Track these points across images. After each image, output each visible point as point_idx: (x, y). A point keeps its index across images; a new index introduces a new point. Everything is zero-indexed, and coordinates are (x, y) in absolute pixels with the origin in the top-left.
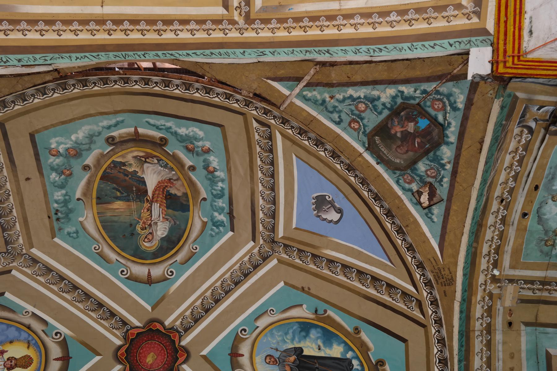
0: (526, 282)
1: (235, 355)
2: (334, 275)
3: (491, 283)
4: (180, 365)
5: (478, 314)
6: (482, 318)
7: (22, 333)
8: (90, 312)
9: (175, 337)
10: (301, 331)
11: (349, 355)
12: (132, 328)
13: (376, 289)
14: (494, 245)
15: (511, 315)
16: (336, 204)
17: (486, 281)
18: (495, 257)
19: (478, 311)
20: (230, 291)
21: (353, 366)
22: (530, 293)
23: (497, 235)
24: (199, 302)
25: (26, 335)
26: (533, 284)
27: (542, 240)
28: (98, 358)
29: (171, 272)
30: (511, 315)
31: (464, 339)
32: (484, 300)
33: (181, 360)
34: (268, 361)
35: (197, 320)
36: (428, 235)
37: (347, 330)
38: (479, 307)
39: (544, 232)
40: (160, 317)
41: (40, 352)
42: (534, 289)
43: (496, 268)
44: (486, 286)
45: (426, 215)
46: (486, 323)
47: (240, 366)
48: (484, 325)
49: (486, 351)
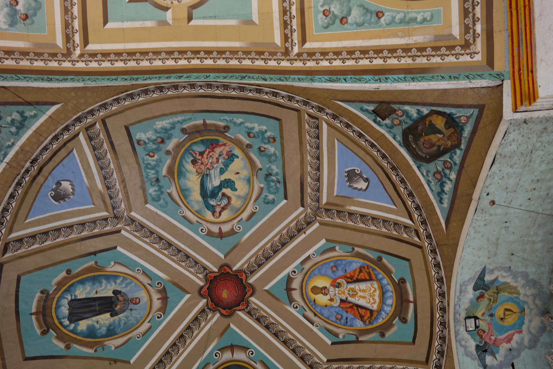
1: (164, 299)
4: (205, 285)
7: (319, 311)
8: (274, 322)
9: (212, 305)
11: (72, 326)
12: (244, 310)
20: (172, 346)
21: (68, 320)
24: (196, 333)
25: (316, 309)
28: (267, 288)
29: (216, 356)
33: (205, 289)
34: (138, 300)
35: (196, 319)
37: (76, 343)
40: (223, 319)
41: (307, 296)
47: (159, 292)
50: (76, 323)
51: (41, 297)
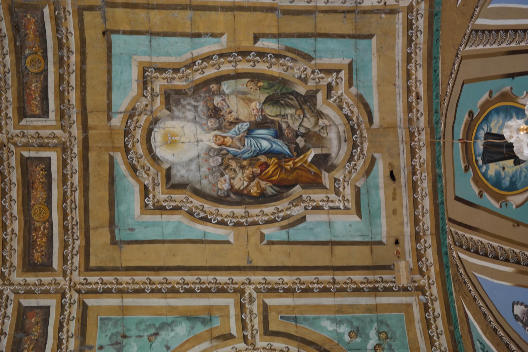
0: (390, 289)
2: (501, 246)
3: (424, 287)
5: (430, 252)
6: (425, 248)
10: (516, 181)
11: (484, 167)
13: (474, 241)
14: (434, 330)
15: (398, 252)
16: (521, 325)
17: (430, 288)
18: (428, 316)
19: (430, 255)
22: (386, 277)
23: (435, 341)
26: (384, 287)
27: (391, 338)
30: (398, 252)
31: (441, 226)
32: (427, 267)
36: (475, 324)
37: (487, 192)
38: (431, 260)
39: (393, 348)
42: (383, 282)
43: (424, 303)
44: (428, 282)
45: (484, 346)
46: (421, 243)
48: (422, 241)
49: (419, 215)
50: (487, 164)
51: (467, 121)
